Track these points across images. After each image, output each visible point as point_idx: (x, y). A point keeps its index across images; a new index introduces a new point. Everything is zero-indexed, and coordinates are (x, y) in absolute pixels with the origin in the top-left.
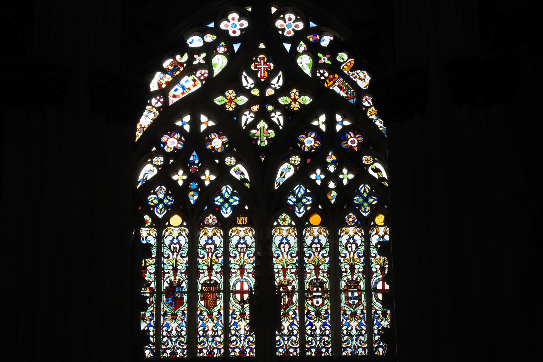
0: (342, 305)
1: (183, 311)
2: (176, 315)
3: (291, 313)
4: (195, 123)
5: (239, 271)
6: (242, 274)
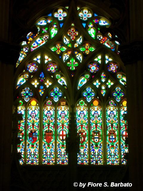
0: (107, 142)
1: (37, 144)
3: (84, 145)
4: (43, 59)
5: (61, 126)
6: (63, 127)
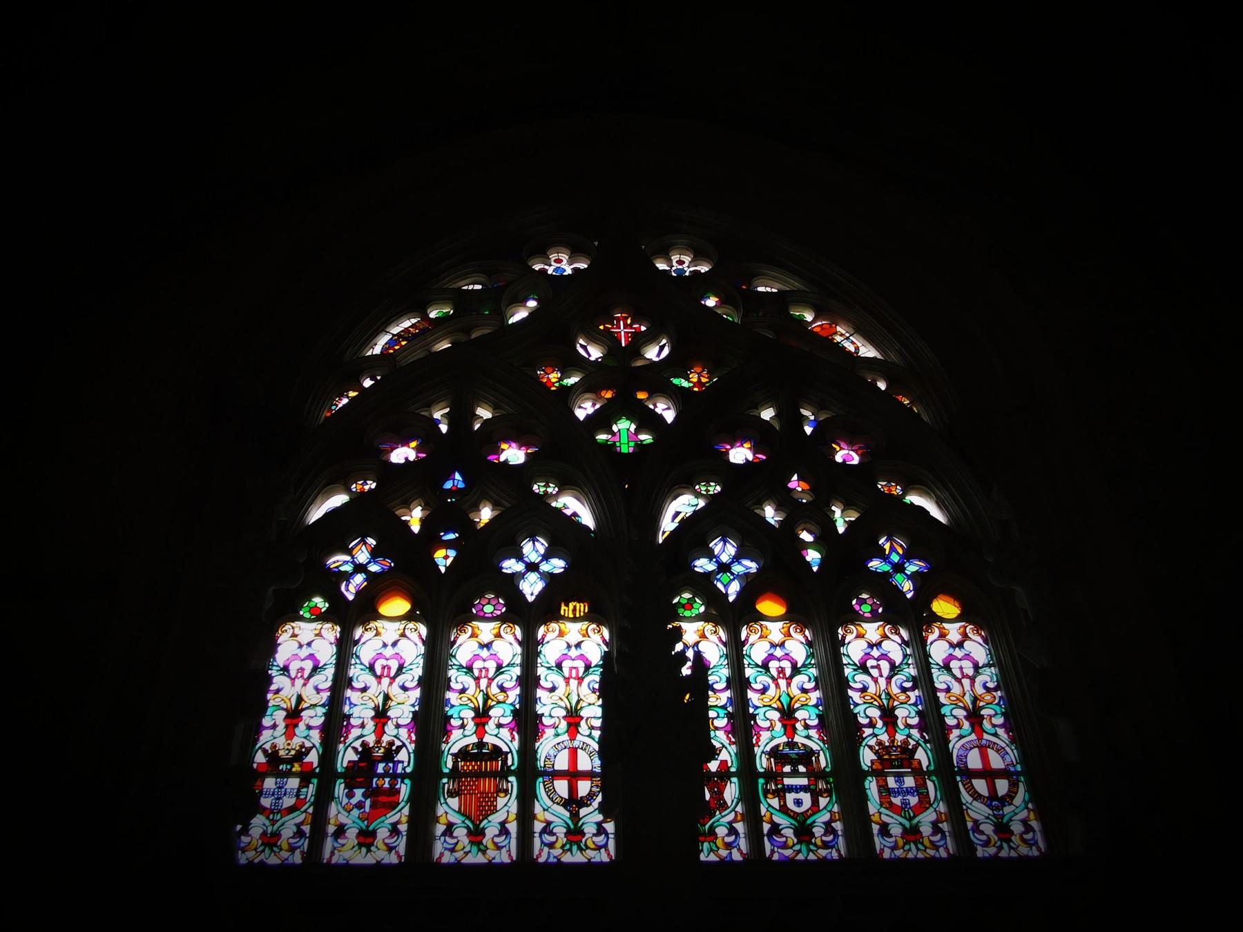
2: (373, 834)
3: (721, 831)
5: (563, 725)
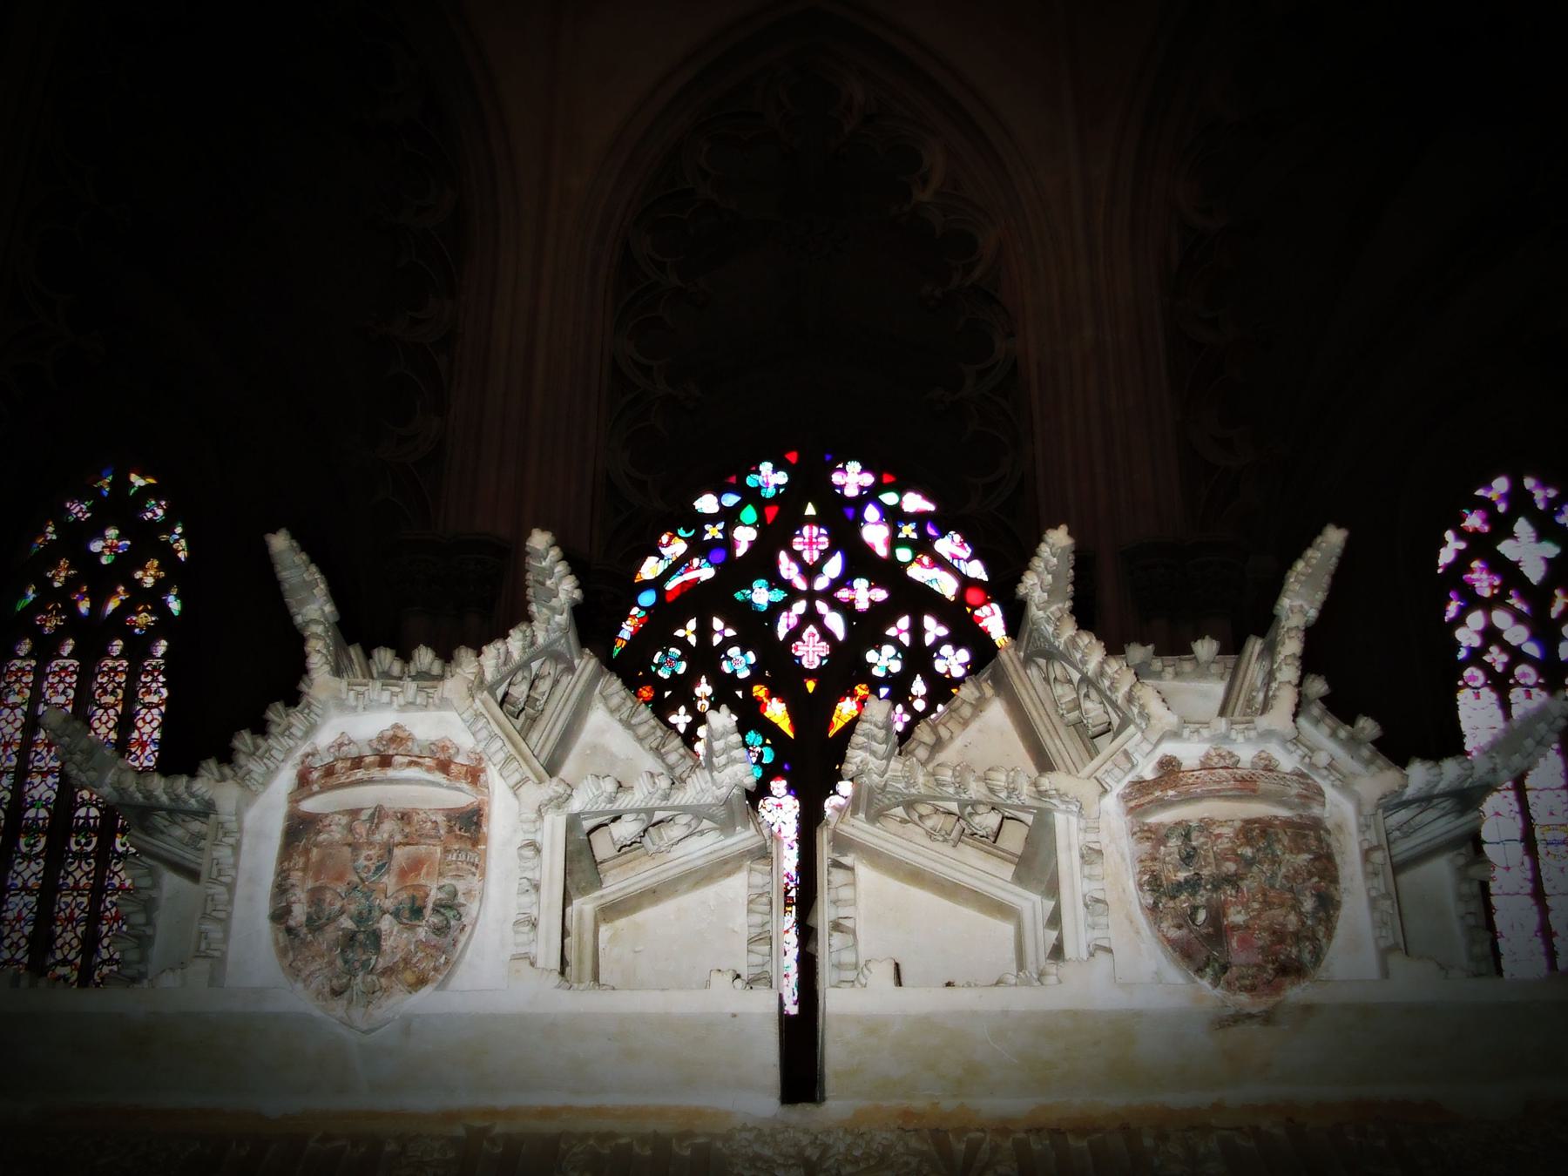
4: (704, 631)
